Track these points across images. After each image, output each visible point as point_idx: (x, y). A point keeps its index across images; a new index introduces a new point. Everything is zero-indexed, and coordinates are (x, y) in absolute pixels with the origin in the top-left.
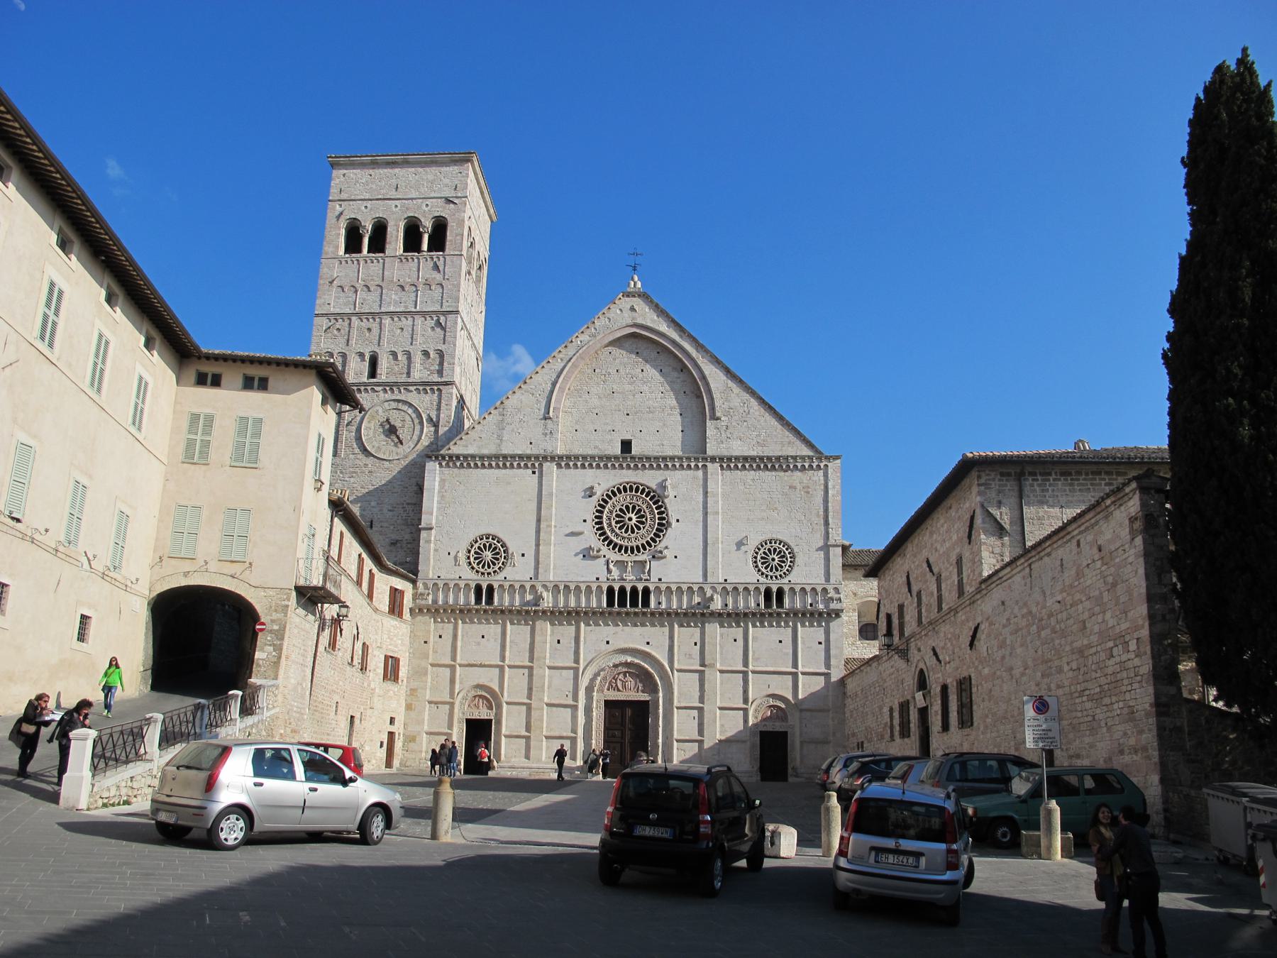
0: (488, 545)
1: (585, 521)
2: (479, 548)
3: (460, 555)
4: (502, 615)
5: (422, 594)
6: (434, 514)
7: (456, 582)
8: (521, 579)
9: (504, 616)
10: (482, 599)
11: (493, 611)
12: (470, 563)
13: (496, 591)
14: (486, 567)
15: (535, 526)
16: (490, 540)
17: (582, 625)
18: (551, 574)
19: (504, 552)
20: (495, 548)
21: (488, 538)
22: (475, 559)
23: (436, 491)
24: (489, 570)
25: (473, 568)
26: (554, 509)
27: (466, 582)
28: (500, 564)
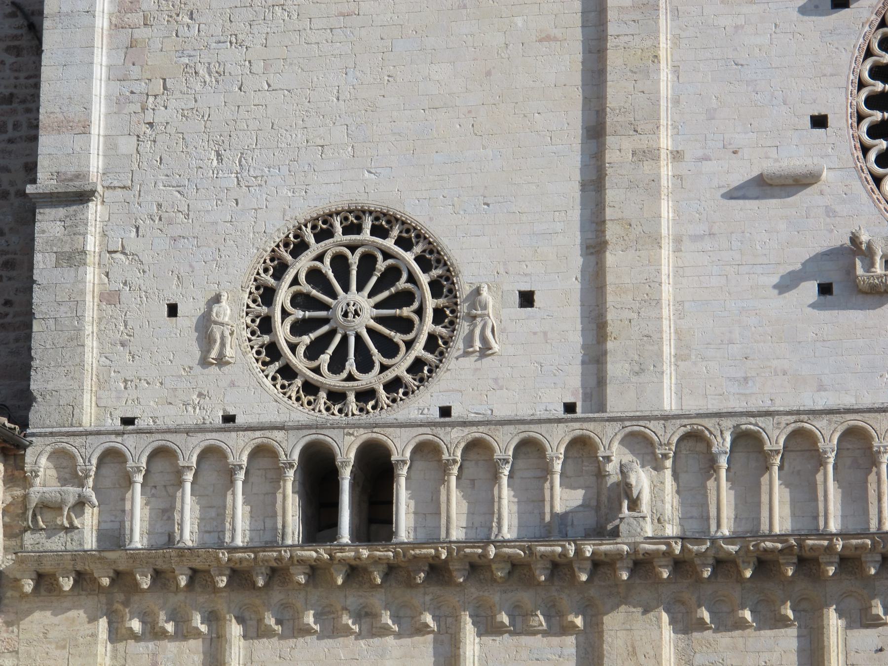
0: (354, 260)
1: (819, 122)
2: (315, 276)
3: (225, 311)
4: (435, 590)
5: (48, 507)
6: (98, 126)
7: (212, 439)
8: (524, 412)
9: (452, 597)
10: (333, 524)
11: (391, 570)
12: (272, 351)
13: (404, 471)
14: (351, 365)
15: (576, 160)
16: (366, 235)
17: (833, 621)
18: (669, 382)
19: (436, 294)
20: (392, 274)
21: (356, 229)
22: (299, 328)
23: (102, 22)
24: (366, 380)
25: (288, 372)
26: (665, 75)
27: (258, 437)
28: (419, 350)
